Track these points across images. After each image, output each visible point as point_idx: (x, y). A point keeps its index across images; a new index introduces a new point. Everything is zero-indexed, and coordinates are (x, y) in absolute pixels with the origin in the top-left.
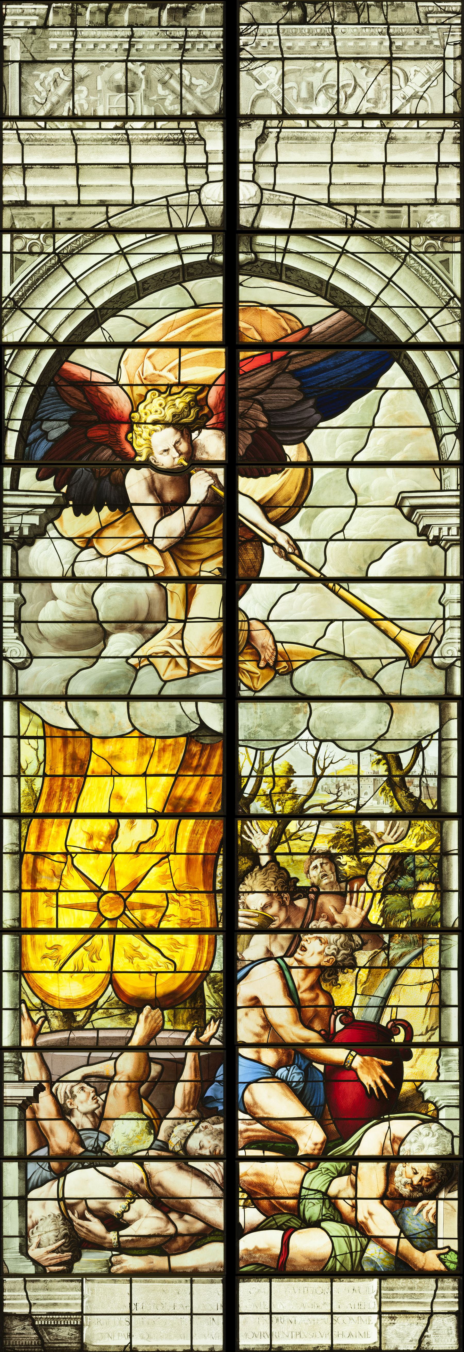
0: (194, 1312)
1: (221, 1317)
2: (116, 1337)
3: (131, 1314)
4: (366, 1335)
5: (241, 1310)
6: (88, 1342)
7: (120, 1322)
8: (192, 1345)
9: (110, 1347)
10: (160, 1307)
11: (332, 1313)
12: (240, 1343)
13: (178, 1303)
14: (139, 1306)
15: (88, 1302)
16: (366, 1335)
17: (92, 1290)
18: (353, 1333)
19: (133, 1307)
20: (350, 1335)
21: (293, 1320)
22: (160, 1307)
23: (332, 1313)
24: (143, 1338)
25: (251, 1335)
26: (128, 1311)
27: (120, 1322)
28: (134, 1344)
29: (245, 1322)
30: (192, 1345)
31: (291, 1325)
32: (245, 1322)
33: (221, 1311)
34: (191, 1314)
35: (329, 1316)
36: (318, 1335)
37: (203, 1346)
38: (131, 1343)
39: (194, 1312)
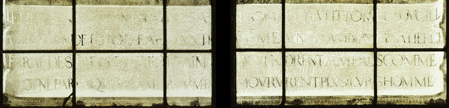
0: (169, 47)
1: (209, 56)
2: (52, 86)
3: (74, 51)
4: (427, 82)
5: (240, 44)
6: (10, 93)
7: (58, 63)
8: (165, 98)
9: (42, 99)
10: (117, 41)
11: (375, 50)
12: (238, 95)
13: (145, 34)
14: (87, 39)
15: (10, 33)
16: (427, 82)
17: (16, 14)
18: (407, 79)
19: (78, 40)
20: (403, 82)
21: (317, 60)
22: (117, 41)
23: (375, 50)
24: (92, 87)
25: (253, 82)
26: (69, 46)
27: (58, 63)
28: (79, 95)
29: (245, 62)
30: (165, 98)
31: (314, 68)
32: (245, 62)
33: (209, 46)
34: (165, 51)
35: (371, 54)
36: (355, 82)
37: (182, 99)
38: (74, 93)
39: (169, 47)
